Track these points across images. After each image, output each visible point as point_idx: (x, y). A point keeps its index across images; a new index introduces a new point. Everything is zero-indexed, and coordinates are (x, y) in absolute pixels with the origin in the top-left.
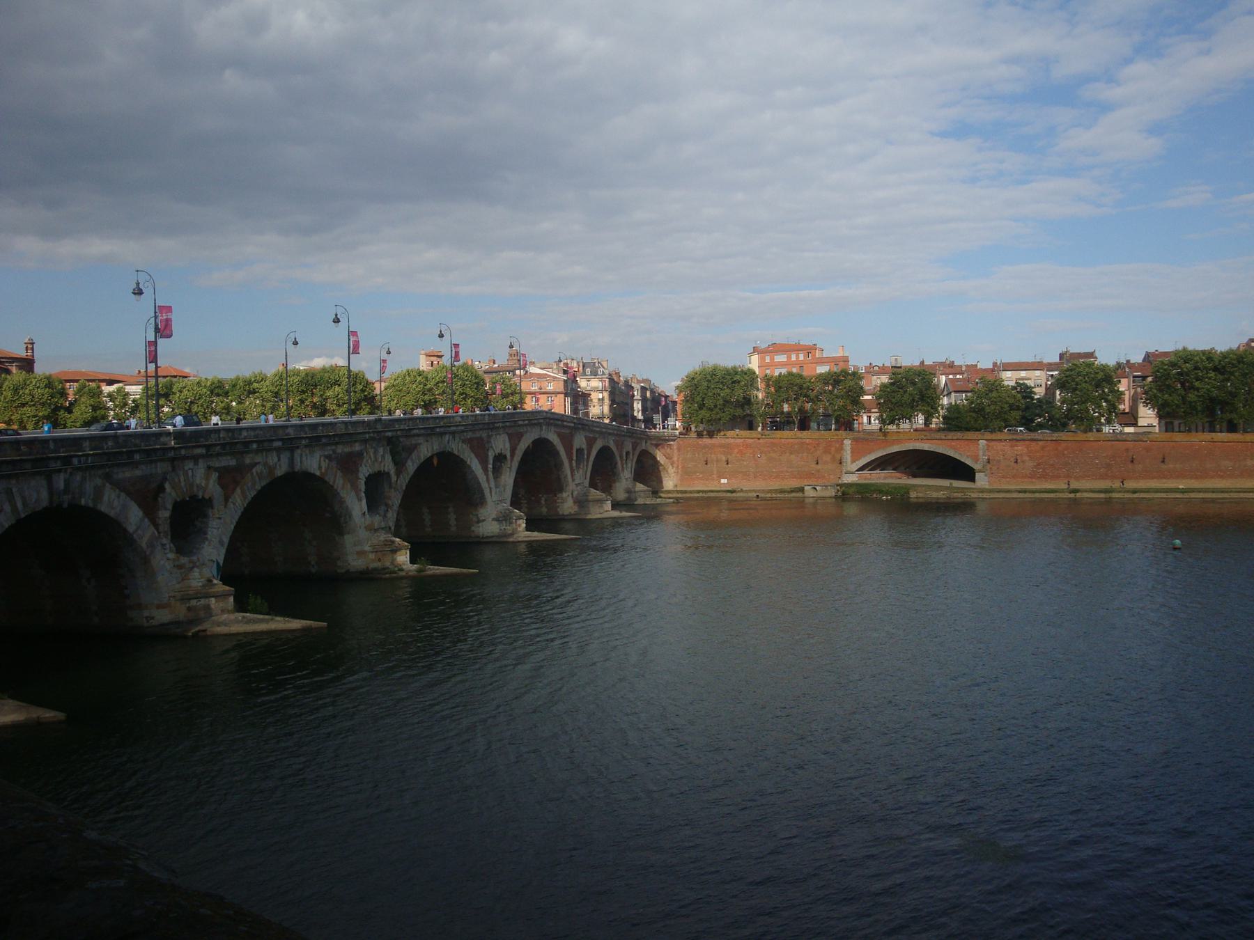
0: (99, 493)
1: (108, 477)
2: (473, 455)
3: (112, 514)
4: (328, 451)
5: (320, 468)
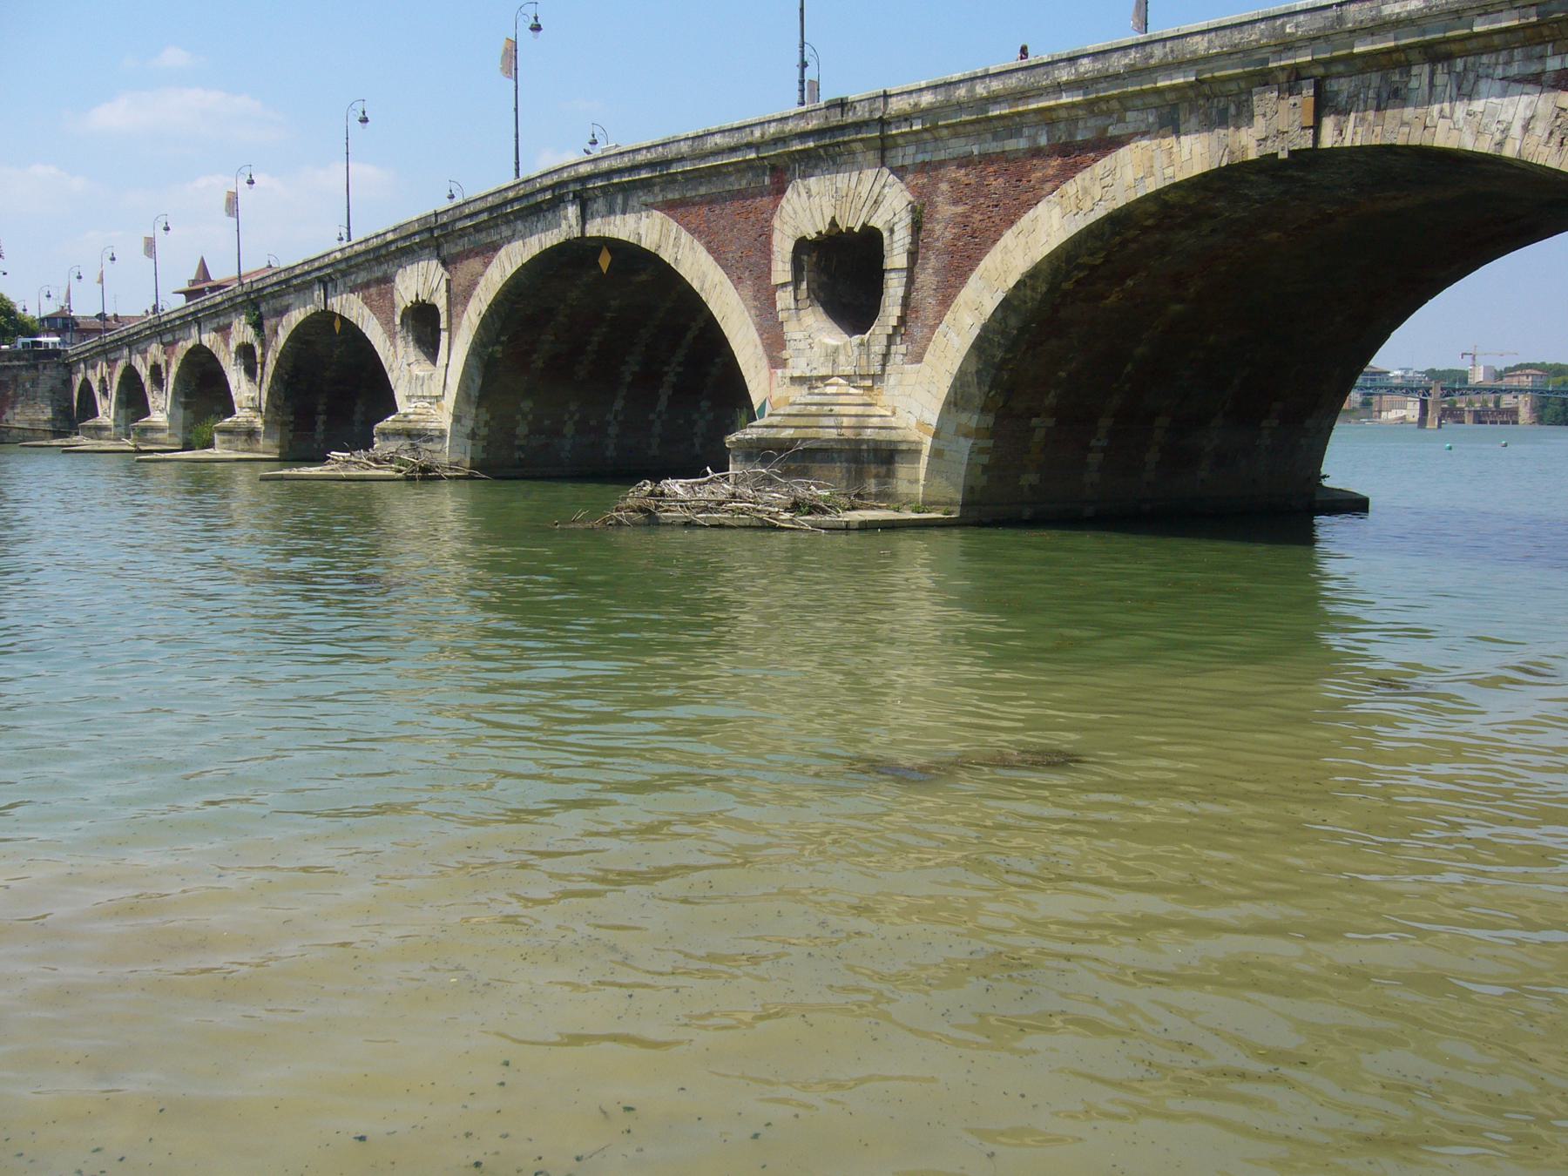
2: (367, 311)
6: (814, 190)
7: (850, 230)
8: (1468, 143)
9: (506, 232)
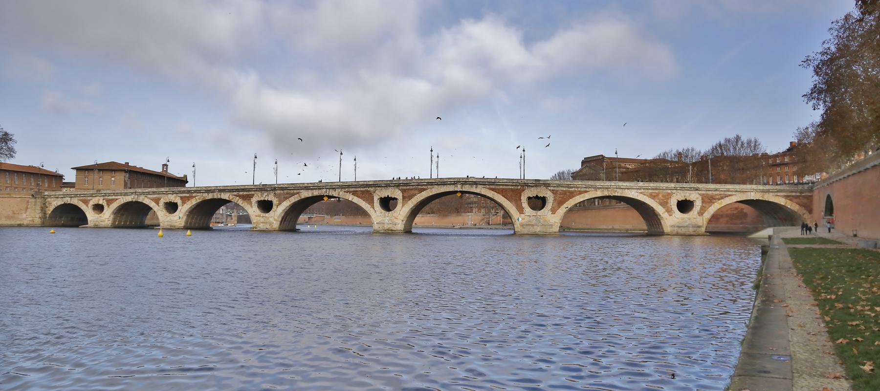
0: (143, 199)
1: (146, 196)
3: (146, 203)
4: (235, 193)
5: (229, 198)
6: (532, 190)
7: (541, 197)
8: (632, 197)
9: (429, 187)
